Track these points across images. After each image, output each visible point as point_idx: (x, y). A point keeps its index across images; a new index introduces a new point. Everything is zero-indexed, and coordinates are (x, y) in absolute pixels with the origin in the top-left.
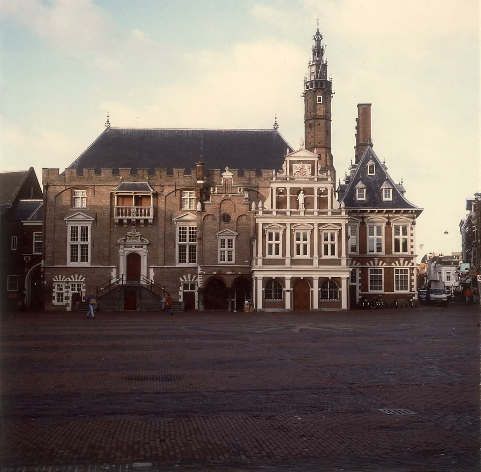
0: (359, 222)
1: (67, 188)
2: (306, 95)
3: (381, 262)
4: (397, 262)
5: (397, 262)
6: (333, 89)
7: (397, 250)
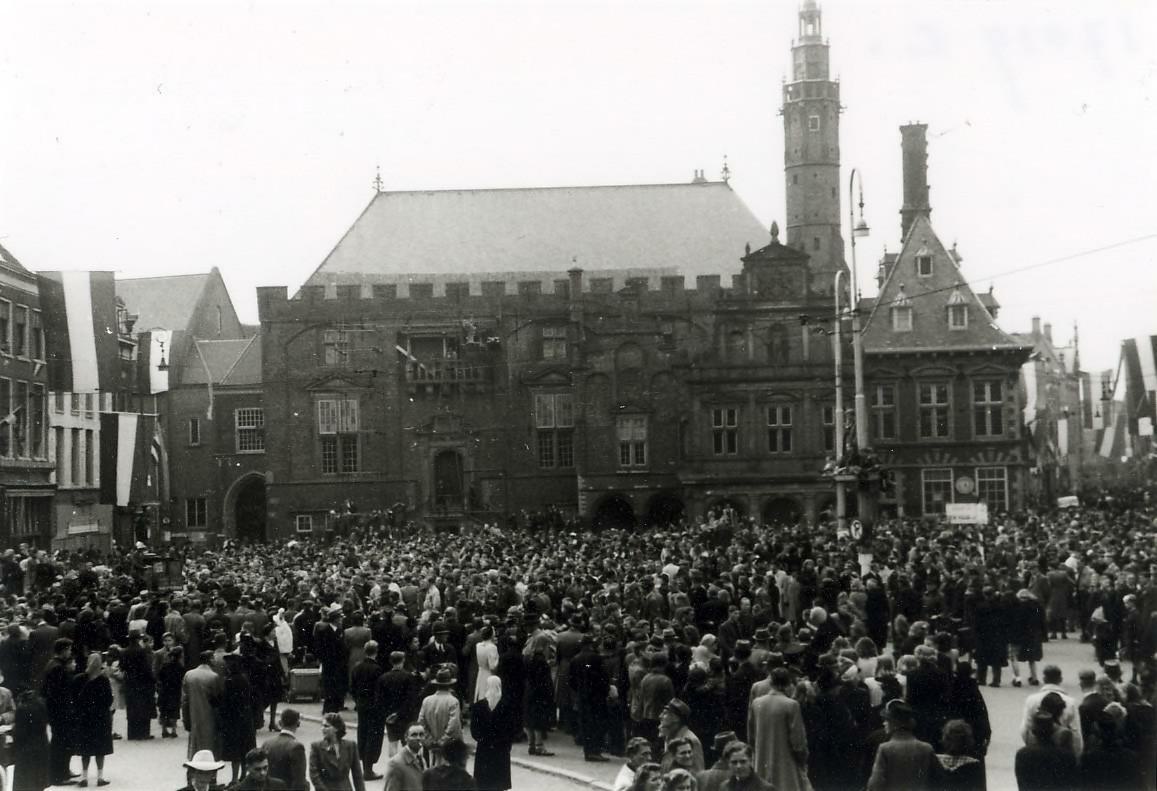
0: (897, 378)
1: (311, 325)
2: (787, 112)
3: (947, 456)
4: (980, 455)
5: (980, 455)
6: (844, 98)
7: (981, 430)
